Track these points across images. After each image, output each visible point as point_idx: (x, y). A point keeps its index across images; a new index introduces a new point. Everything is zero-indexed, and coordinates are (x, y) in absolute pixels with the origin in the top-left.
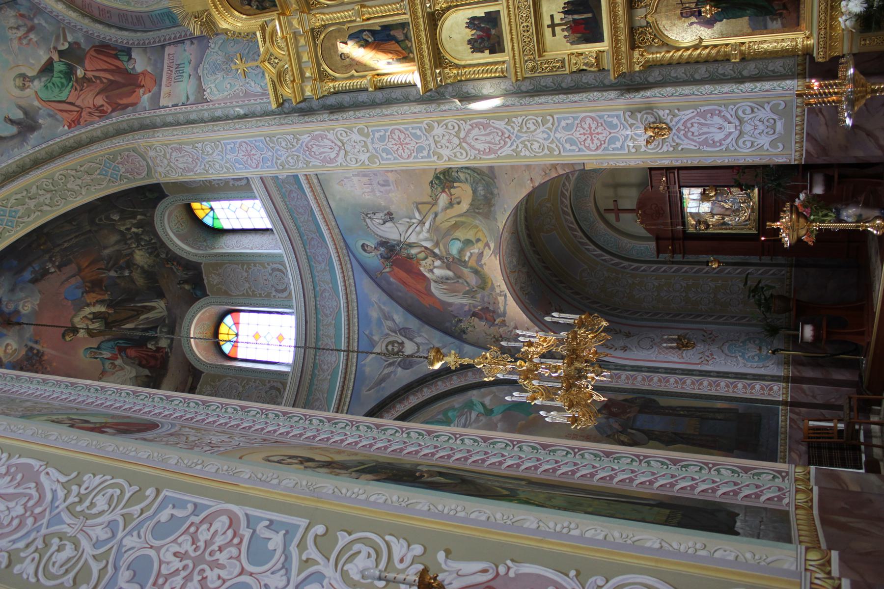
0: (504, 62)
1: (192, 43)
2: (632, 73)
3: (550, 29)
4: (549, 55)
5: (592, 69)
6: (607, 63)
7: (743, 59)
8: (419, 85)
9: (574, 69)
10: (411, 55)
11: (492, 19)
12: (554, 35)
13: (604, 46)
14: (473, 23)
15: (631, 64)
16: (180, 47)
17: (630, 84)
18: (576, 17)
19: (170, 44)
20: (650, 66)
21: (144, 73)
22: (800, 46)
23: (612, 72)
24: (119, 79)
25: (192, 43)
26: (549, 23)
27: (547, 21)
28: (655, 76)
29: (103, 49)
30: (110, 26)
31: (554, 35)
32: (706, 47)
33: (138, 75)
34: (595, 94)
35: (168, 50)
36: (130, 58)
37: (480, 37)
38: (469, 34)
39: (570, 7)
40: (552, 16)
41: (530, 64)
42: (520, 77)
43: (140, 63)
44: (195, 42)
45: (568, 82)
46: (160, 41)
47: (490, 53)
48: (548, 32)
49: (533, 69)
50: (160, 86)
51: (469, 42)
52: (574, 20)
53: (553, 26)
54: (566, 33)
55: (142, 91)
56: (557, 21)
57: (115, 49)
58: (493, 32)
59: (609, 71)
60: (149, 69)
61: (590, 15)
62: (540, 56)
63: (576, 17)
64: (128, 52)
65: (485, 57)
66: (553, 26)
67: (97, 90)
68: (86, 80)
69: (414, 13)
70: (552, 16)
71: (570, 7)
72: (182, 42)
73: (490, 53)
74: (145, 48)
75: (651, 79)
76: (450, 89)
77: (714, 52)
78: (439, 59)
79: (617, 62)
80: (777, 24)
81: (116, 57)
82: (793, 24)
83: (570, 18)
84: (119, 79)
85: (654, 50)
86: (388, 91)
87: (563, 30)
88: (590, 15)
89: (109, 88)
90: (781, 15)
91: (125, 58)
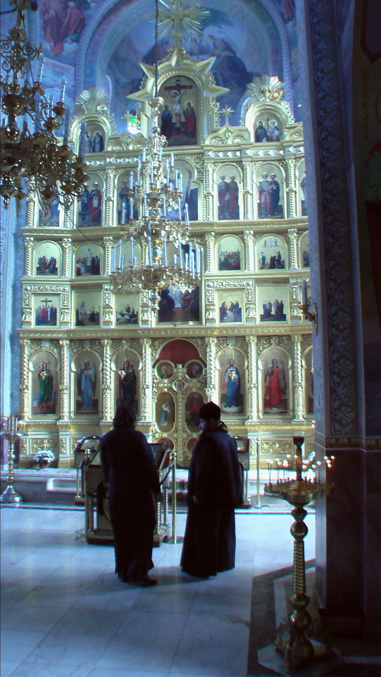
0: (32, 274)
1: (73, 86)
2: (19, 338)
3: (44, 300)
4: (33, 298)
5: (23, 319)
6: (25, 327)
7: (21, 390)
8: (27, 227)
9: (24, 310)
10: (42, 224)
11: (54, 271)
12: (42, 301)
13: (33, 326)
14: (53, 261)
15: (23, 338)
16: (72, 78)
17: (14, 338)
18: (49, 313)
19: (76, 71)
20: (22, 347)
21: (62, 48)
22: (24, 414)
23: (20, 329)
24: (63, 29)
25: (73, 86)
26: (48, 300)
27: (49, 298)
28: (16, 348)
29: (82, 24)
30: (94, 33)
31: (42, 301)
32: (28, 373)
33: (62, 44)
34: (11, 319)
35: (73, 68)
36: (73, 41)
37: (46, 263)
38: (48, 258)
39: (54, 311)
40: (51, 301)
41: (29, 288)
42: (23, 282)
43: (69, 47)
44: (74, 89)
45: (18, 305)
46: (79, 65)
47: (37, 268)
48: (43, 298)
49: (26, 289)
50: (53, 59)
51: (44, 257)
52: (47, 312)
53: (46, 301)
54: (42, 307)
55: (52, 44)
56: (48, 303)
57: (81, 32)
58: (47, 270)
59: (21, 327)
60: (64, 53)
61: (49, 320)
62: (32, 293)
63: (49, 313)
64: (77, 40)
65: (36, 265)
66: (46, 301)
67: (59, 13)
68: (66, 7)
69: (62, 231)
70: (51, 301)
71: (54, 311)
72: (75, 80)
73: (38, 269)
74: (77, 53)
75: (15, 347)
76: (22, 243)
77: (25, 377)
78: (39, 239)
79: (25, 332)
80: (35, 404)
81: (75, 32)
82: (35, 412)
83: (49, 310)
84: (63, 29)
85: (29, 349)
86: (25, 207)
87: (43, 306)
88: (49, 320)
89: (58, 21)
90: (39, 406)
91: (74, 38)
